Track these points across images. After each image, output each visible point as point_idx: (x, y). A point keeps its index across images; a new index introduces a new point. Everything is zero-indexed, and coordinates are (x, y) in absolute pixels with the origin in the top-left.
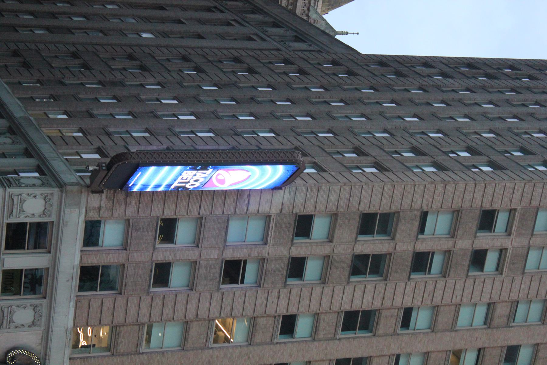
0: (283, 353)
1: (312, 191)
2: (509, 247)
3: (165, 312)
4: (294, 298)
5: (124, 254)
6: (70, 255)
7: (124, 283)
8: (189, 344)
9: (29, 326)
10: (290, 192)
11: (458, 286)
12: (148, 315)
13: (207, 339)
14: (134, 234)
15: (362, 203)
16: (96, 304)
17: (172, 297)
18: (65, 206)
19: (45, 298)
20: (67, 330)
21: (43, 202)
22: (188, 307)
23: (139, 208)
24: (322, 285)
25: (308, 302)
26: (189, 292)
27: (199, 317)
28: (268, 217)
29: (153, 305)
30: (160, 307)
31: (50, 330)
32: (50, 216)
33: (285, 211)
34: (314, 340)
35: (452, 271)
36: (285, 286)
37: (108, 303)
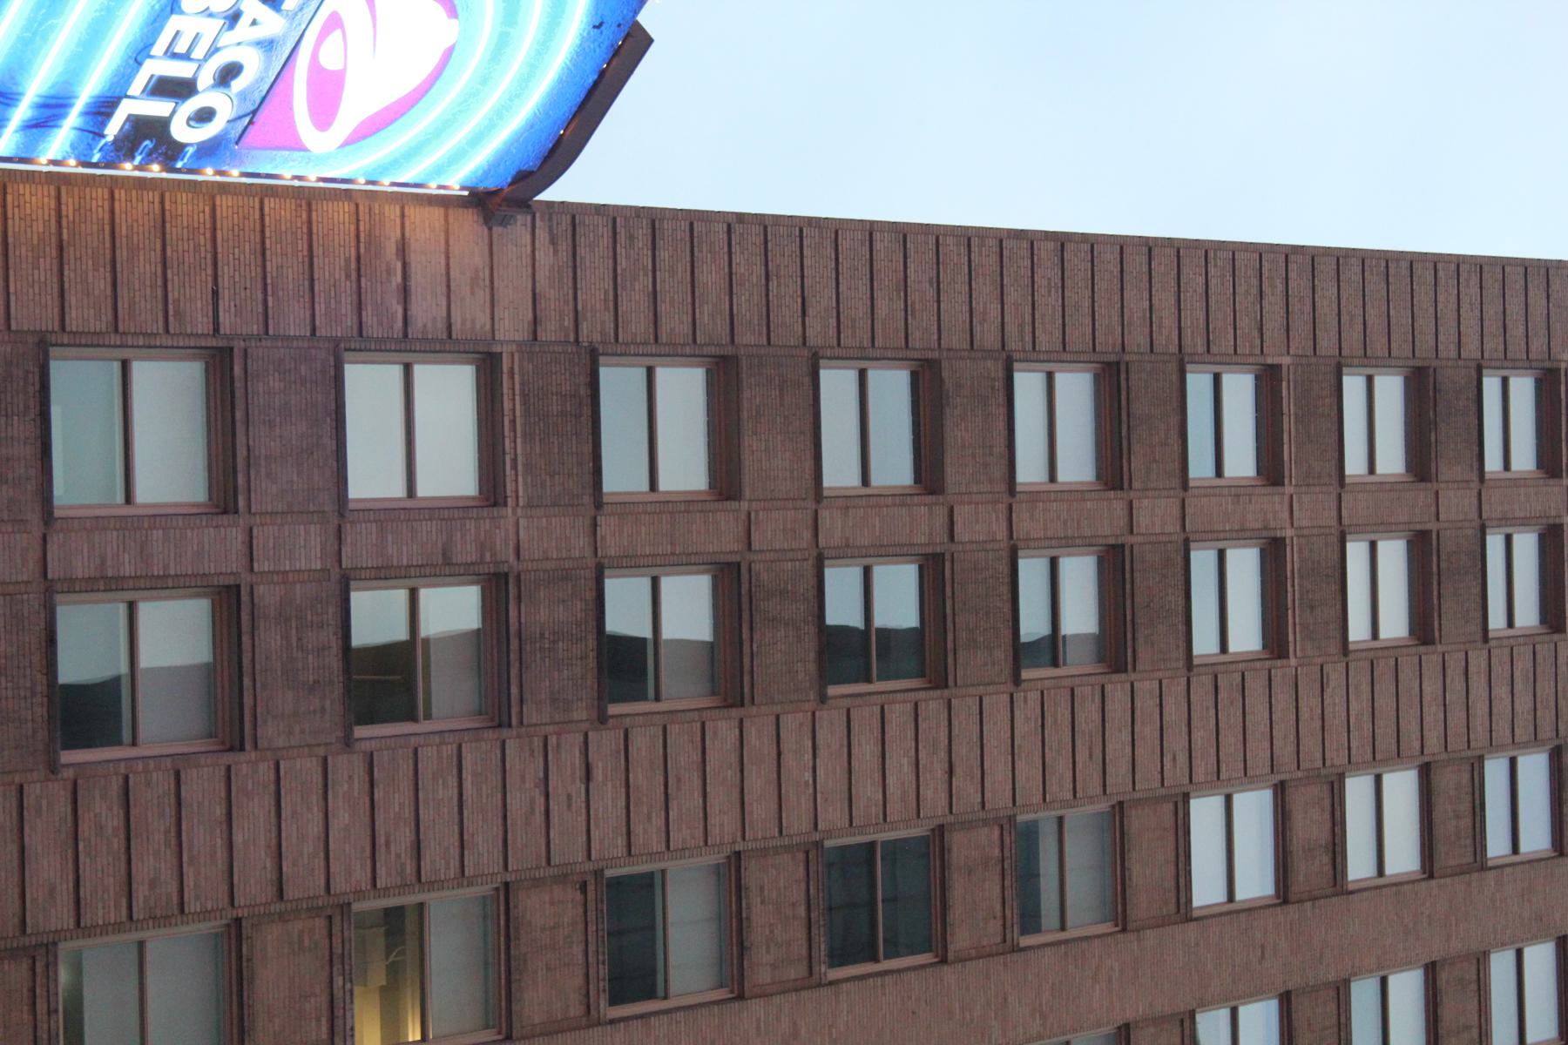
1: (631, 238)
2: (1289, 533)
3: (144, 868)
10: (553, 241)
15: (810, 311)
17: (162, 782)
22: (238, 839)
24: (735, 712)
25: (697, 795)
27: (290, 893)
29: (85, 829)
30: (117, 844)
33: (550, 331)
34: (741, 997)
35: (1141, 641)
36: (602, 719)
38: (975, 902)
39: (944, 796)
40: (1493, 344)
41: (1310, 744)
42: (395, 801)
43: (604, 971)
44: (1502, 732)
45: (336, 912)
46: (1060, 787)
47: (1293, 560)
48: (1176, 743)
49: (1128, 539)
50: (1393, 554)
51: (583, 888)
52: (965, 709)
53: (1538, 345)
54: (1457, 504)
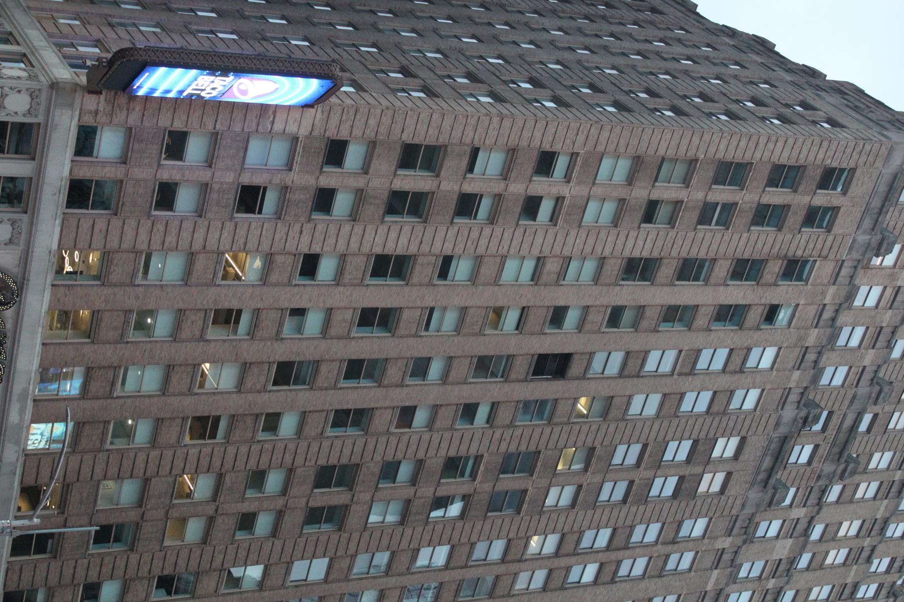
0: (301, 297)
3: (168, 239)
4: (319, 236)
5: (123, 168)
6: (59, 166)
8: (193, 280)
9: (5, 244)
10: (323, 112)
11: (506, 235)
14: (136, 146)
16: (86, 225)
17: (177, 223)
18: (55, 106)
19: (26, 212)
20: (50, 252)
21: (28, 99)
22: (195, 236)
24: (352, 223)
26: (197, 219)
27: (207, 248)
28: (295, 140)
30: (162, 234)
32: (36, 116)
33: (316, 133)
34: (338, 285)
35: (501, 217)
36: (309, 220)
37: (101, 224)
49: (504, 193)
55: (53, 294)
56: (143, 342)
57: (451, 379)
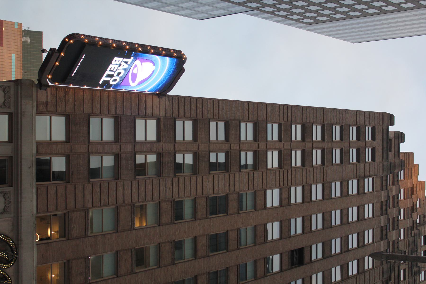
1: (181, 101)
2: (283, 149)
3: (103, 197)
7: (71, 173)
8: (120, 228)
10: (169, 101)
12: (91, 200)
13: (132, 222)
15: (209, 113)
16: (52, 191)
17: (106, 184)
19: (12, 186)
20: (33, 215)
22: (118, 193)
23: (75, 105)
25: (190, 188)
27: (126, 202)
29: (94, 192)
30: (99, 194)
31: (20, 215)
32: (9, 107)
33: (168, 115)
34: (196, 220)
36: (175, 176)
37: (61, 190)
38: (233, 206)
39: (228, 189)
40: (315, 120)
41: (285, 182)
42: (142, 188)
43: (174, 215)
44: (315, 181)
45: (133, 205)
46: (246, 188)
47: (283, 153)
48: (265, 181)
49: (258, 150)
50: (299, 153)
51: (171, 202)
52: (232, 175)
53: (322, 120)
54: (309, 145)
55: (39, 252)
56: (100, 281)
57: (258, 276)
